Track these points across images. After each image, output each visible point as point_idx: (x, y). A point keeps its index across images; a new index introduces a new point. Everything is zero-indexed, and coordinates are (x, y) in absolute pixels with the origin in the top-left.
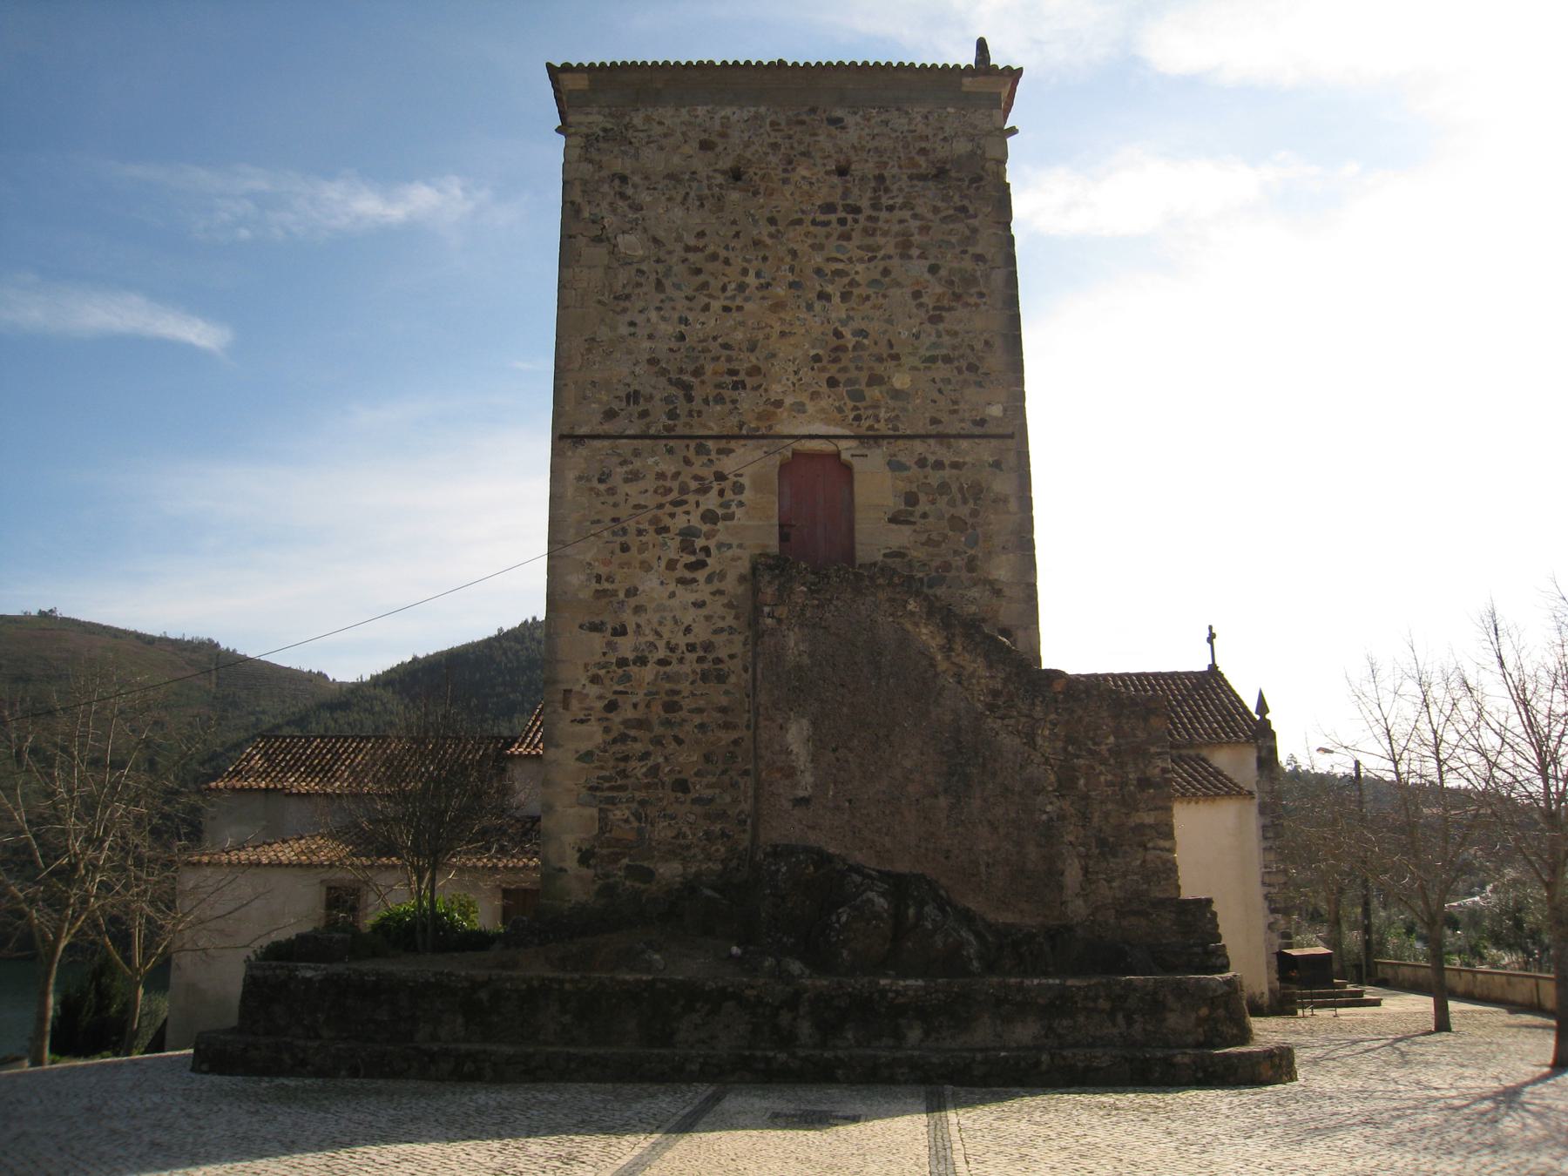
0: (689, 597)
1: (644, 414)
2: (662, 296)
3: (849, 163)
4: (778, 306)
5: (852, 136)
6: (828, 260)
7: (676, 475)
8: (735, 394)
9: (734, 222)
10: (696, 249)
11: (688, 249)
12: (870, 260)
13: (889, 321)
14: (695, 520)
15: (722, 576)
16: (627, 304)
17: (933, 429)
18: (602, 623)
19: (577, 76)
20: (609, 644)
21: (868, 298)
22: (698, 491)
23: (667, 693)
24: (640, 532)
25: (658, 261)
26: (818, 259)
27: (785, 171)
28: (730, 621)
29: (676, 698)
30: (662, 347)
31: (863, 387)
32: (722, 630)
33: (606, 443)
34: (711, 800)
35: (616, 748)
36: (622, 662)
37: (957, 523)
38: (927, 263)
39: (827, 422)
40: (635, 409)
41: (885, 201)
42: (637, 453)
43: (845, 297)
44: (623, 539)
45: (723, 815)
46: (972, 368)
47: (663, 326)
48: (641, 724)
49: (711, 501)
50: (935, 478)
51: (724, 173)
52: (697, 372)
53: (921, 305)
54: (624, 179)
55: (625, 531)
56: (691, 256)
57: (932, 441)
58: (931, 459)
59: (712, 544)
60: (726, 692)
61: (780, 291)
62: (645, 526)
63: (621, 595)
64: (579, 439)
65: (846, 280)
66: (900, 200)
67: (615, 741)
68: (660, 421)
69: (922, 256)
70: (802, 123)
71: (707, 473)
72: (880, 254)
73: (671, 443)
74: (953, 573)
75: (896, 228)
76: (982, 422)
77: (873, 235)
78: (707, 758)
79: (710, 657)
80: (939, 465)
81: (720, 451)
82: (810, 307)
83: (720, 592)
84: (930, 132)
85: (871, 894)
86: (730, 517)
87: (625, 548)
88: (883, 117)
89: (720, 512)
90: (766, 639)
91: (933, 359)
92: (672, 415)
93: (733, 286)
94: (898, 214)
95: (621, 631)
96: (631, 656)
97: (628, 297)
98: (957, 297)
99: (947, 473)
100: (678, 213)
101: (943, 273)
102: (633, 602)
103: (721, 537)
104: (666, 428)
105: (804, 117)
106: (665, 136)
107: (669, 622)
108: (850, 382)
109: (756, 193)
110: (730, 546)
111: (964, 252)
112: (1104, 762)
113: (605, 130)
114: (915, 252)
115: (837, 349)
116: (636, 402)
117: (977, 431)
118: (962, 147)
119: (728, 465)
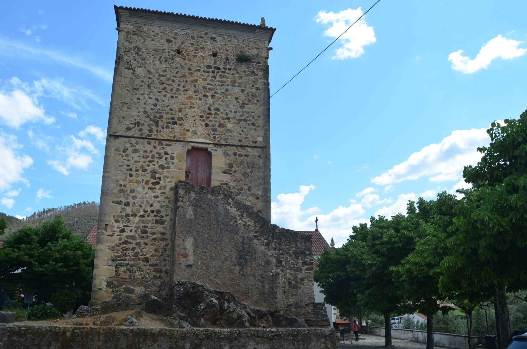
0: (152, 194)
1: (141, 130)
2: (150, 90)
3: (217, 53)
4: (190, 98)
5: (218, 44)
6: (208, 84)
7: (151, 152)
8: (173, 126)
9: (177, 68)
10: (163, 76)
11: (160, 75)
12: (222, 85)
13: (227, 107)
14: (157, 167)
15: (165, 188)
16: (137, 92)
17: (239, 143)
18: (121, 201)
19: (125, 11)
20: (123, 209)
21: (220, 98)
22: (158, 158)
23: (143, 227)
24: (136, 170)
25: (149, 78)
26: (205, 83)
27: (195, 53)
28: (166, 203)
29: (147, 229)
30: (148, 108)
31: (217, 127)
32: (163, 206)
33: (126, 139)
34: (157, 265)
35: (123, 246)
36: (127, 215)
37: (245, 174)
39: (205, 138)
40: (137, 128)
41: (228, 66)
42: (137, 143)
44: (131, 172)
45: (160, 271)
46: (253, 124)
47: (149, 100)
48: (133, 238)
49: (162, 162)
50: (239, 159)
51: (174, 51)
52: (161, 117)
53: (238, 102)
54: (139, 49)
55: (131, 170)
56: (160, 78)
57: (239, 147)
58: (238, 153)
59: (162, 176)
60: (164, 228)
61: (191, 93)
62: (138, 168)
63: (129, 192)
64: (117, 137)
65: (213, 92)
66: (233, 67)
67: (123, 243)
68: (146, 132)
70: (202, 37)
71: (162, 151)
72: (226, 84)
73: (150, 141)
74: (243, 191)
76: (256, 142)
77: (223, 77)
78: (156, 250)
79: (159, 215)
80: (241, 155)
81: (167, 145)
82: (200, 99)
83: (164, 193)
85: (212, 299)
86: (169, 167)
87: (131, 175)
88: (230, 39)
89: (166, 165)
90: (180, 209)
91: (240, 120)
92: (151, 131)
93: (175, 89)
94: (232, 72)
95: (127, 204)
96: (130, 213)
97: (137, 89)
99: (243, 158)
100: (157, 62)
101: (246, 92)
102: (133, 194)
103: (165, 174)
105: (203, 36)
107: (145, 202)
109: (184, 59)
110: (168, 178)
111: (253, 86)
112: (291, 256)
113: (133, 31)
114: (237, 84)
115: (209, 114)
116: (138, 126)
117: (254, 145)
118: (254, 52)
119: (169, 150)
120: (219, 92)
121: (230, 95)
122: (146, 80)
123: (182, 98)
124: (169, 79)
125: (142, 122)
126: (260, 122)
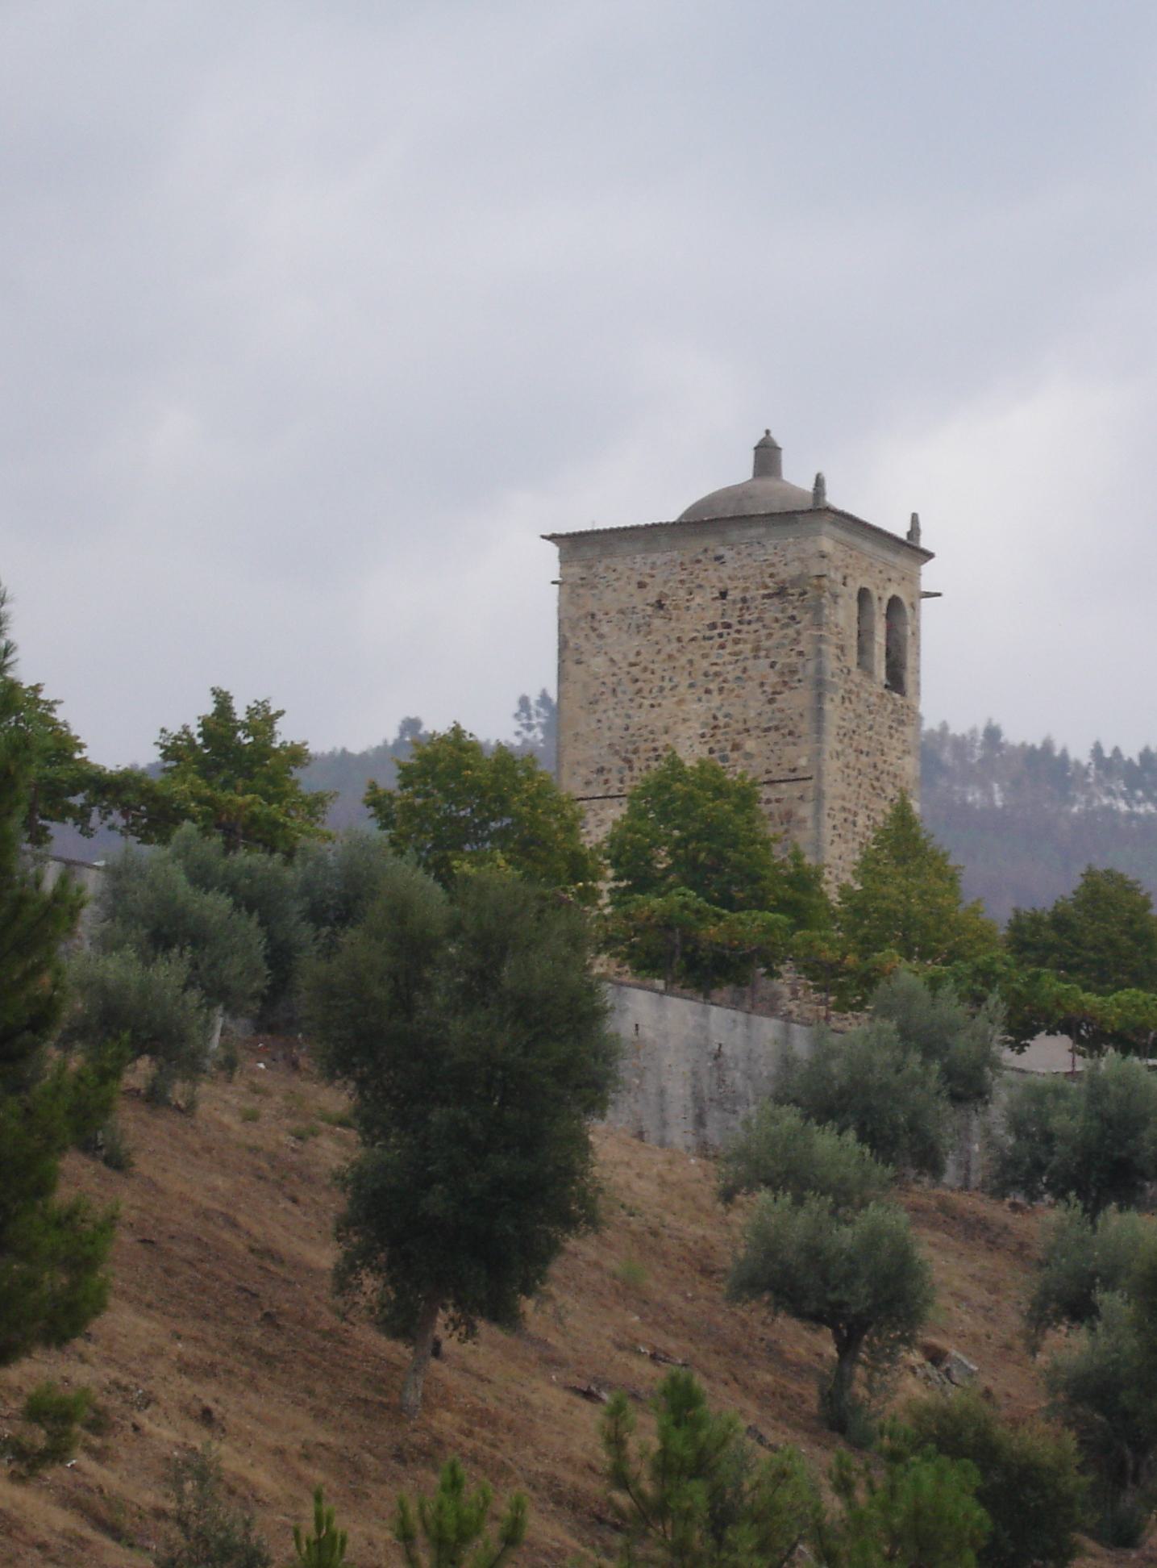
1: (606, 781)
11: (632, 665)
21: (733, 690)
38: (768, 661)
41: (747, 617)
43: (721, 690)
46: (791, 733)
61: (682, 689)
69: (767, 657)
70: (699, 561)
75: (752, 636)
76: (794, 770)
84: (776, 559)
91: (767, 730)
94: (754, 626)
97: (596, 702)
98: (785, 683)
99: (773, 805)
101: (778, 667)
104: (620, 790)
106: (618, 579)
108: (723, 750)
114: (762, 653)
117: (792, 776)
118: (794, 570)
120: (730, 677)
121: (750, 678)
122: (610, 680)
123: (668, 703)
124: (645, 669)
125: (606, 765)
126: (805, 726)
